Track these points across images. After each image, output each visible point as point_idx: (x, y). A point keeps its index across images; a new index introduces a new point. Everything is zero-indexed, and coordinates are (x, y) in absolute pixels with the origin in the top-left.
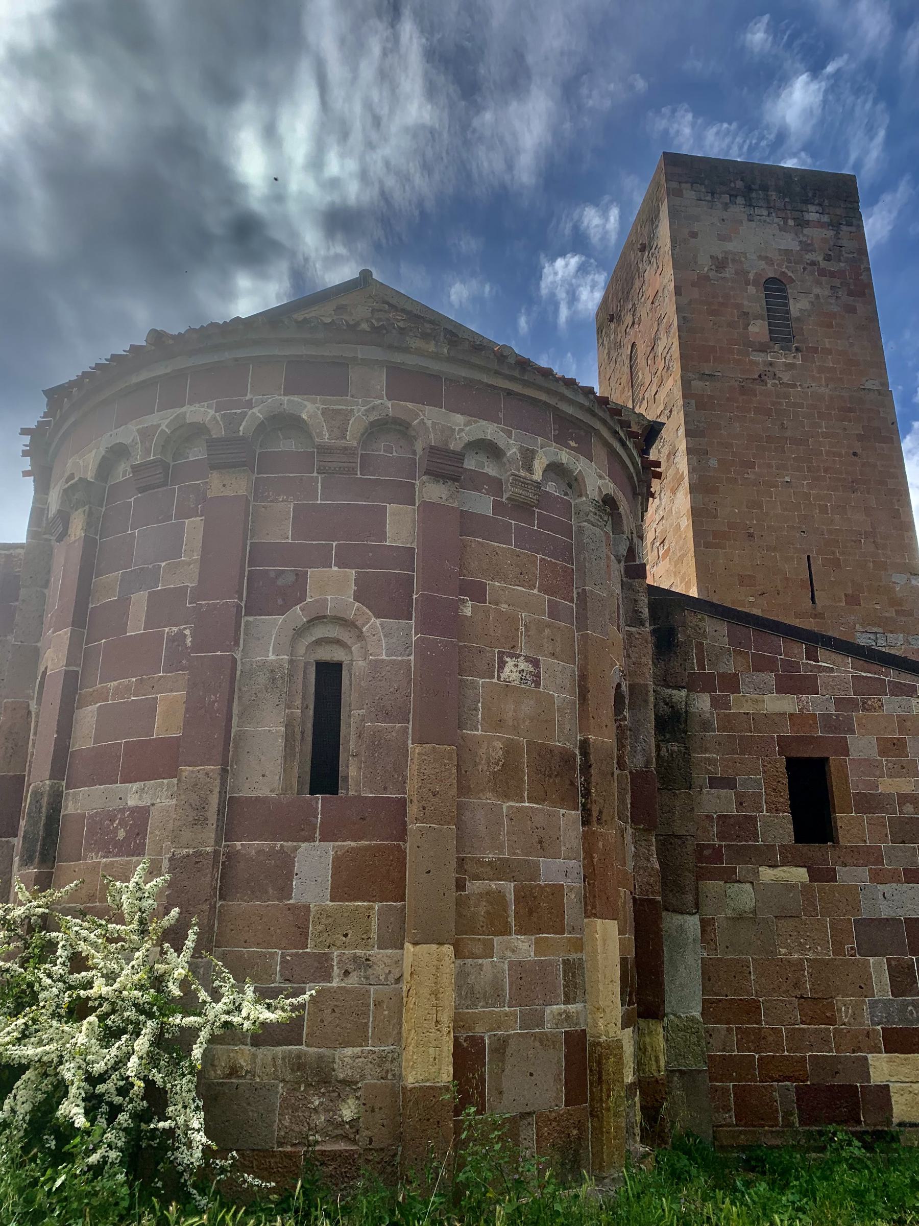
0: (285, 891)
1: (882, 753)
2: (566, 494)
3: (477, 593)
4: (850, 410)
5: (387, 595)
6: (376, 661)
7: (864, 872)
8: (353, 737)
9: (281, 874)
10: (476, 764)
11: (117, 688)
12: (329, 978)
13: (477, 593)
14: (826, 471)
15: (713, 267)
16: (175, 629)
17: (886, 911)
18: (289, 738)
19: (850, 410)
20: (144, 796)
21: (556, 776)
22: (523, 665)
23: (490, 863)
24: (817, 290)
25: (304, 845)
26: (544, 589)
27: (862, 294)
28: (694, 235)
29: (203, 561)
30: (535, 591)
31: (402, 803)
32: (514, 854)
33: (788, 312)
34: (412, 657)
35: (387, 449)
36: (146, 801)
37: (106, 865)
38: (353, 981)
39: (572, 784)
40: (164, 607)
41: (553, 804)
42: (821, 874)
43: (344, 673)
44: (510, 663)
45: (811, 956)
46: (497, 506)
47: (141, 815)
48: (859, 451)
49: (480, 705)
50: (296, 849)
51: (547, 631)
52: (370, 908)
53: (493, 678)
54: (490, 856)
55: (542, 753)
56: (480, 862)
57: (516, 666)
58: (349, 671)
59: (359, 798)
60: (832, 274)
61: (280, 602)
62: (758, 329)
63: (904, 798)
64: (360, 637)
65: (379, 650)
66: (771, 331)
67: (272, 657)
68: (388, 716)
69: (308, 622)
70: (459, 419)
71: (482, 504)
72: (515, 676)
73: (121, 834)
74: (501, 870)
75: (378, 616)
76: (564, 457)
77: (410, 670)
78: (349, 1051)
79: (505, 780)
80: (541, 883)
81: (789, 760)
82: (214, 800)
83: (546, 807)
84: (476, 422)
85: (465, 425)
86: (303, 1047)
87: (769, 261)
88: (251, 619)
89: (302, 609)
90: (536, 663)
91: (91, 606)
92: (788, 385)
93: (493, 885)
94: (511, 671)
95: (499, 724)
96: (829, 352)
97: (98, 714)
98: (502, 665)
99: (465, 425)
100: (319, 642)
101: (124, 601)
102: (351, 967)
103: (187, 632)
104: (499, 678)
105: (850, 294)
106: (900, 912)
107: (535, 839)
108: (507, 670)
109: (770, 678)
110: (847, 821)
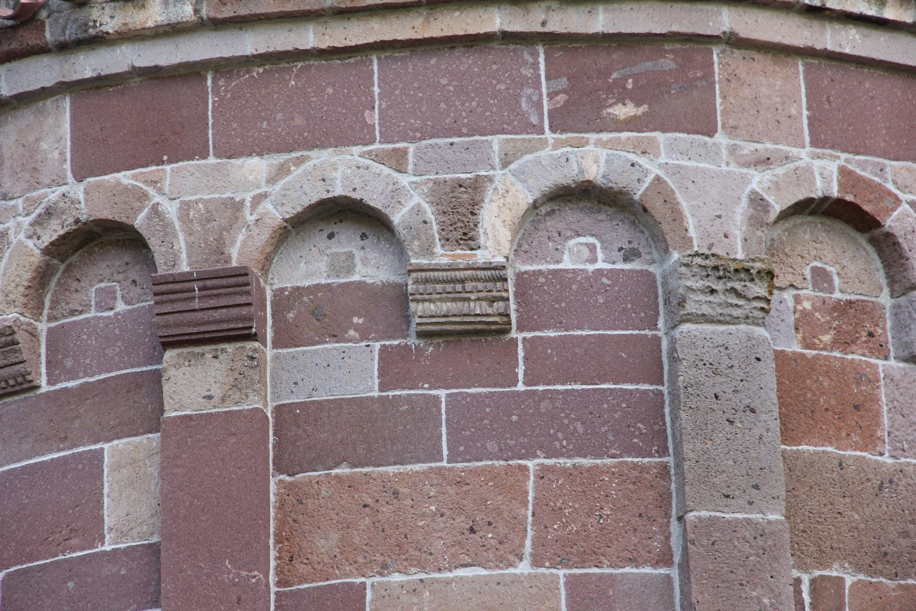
2: (630, 255)
30: (524, 568)
35: (108, 298)
46: (393, 368)
70: (255, 168)
71: (348, 370)
76: (594, 158)
84: (299, 161)
85: (272, 180)
99: (272, 180)
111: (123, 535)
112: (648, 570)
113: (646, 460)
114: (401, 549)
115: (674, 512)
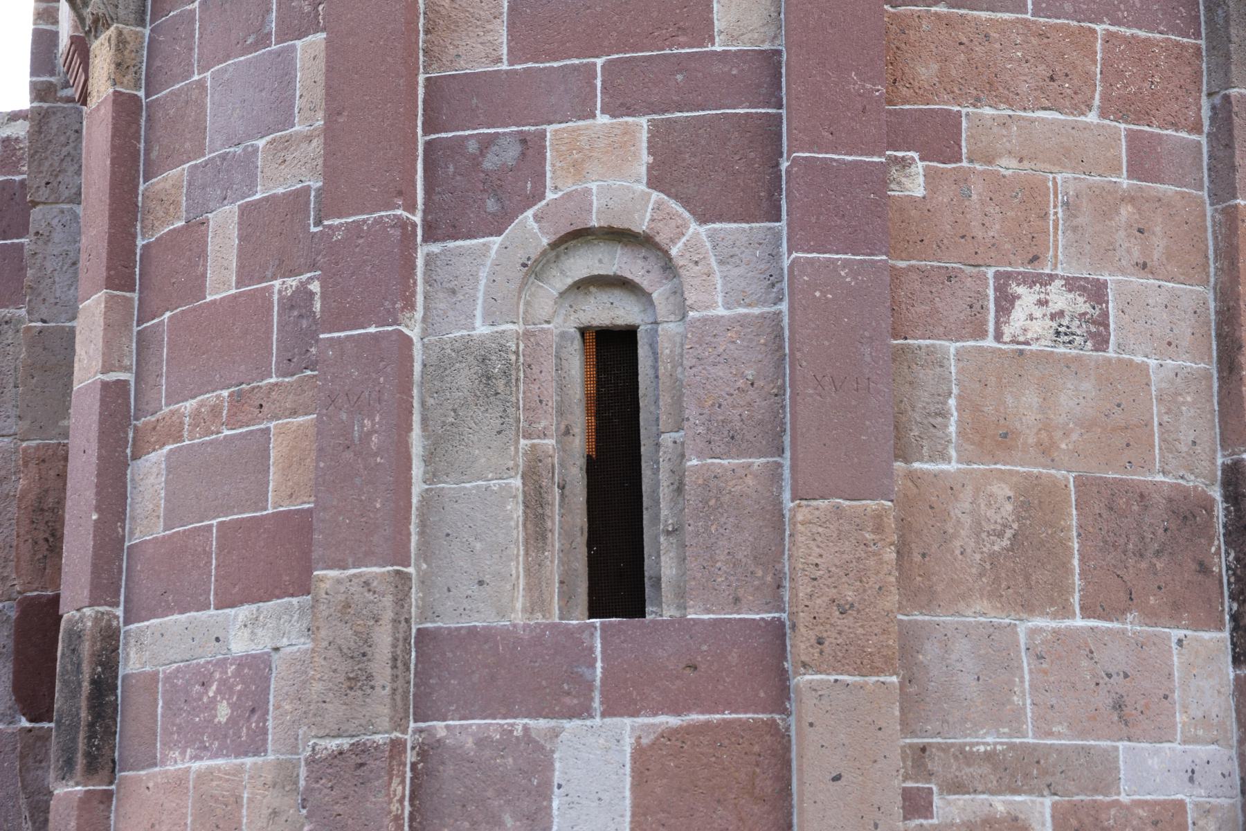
3: (940, 140)
5: (734, 168)
6: (705, 320)
8: (665, 492)
10: (946, 538)
11: (196, 414)
13: (940, 140)
16: (293, 282)
18: (535, 504)
20: (260, 632)
21: (1158, 553)
22: (1060, 299)
23: (989, 757)
25: (571, 726)
26: (1115, 108)
29: (330, 133)
30: (1092, 117)
31: (777, 632)
32: (1050, 734)
34: (784, 307)
37: (200, 776)
39: (1204, 569)
40: (274, 233)
41: (1151, 616)
43: (643, 351)
44: (1027, 297)
47: (256, 670)
49: (952, 402)
50: (555, 734)
51: (1126, 211)
53: (983, 334)
54: (988, 740)
55: (1112, 505)
56: (966, 756)
57: (1042, 303)
58: (653, 346)
59: (682, 624)
61: (491, 205)
64: (669, 267)
65: (712, 292)
67: (482, 329)
68: (734, 442)
69: (554, 245)
72: (1041, 327)
73: (223, 712)
74: (1016, 770)
75: (703, 219)
77: (780, 336)
79: (1025, 569)
80: (1124, 798)
82: (383, 639)
83: (1131, 625)
88: (435, 248)
89: (537, 218)
90: (1096, 292)
91: (140, 242)
93: (1000, 804)
94: (1029, 318)
95: (994, 438)
97: (169, 470)
98: (1006, 303)
100: (586, 284)
101: (196, 226)
103: (315, 287)
104: (998, 337)
107: (1103, 700)
108: (1018, 316)
111: (734, 39)
112: (1184, 135)
113: (1185, 40)
114: (992, 87)
115: (1204, 88)
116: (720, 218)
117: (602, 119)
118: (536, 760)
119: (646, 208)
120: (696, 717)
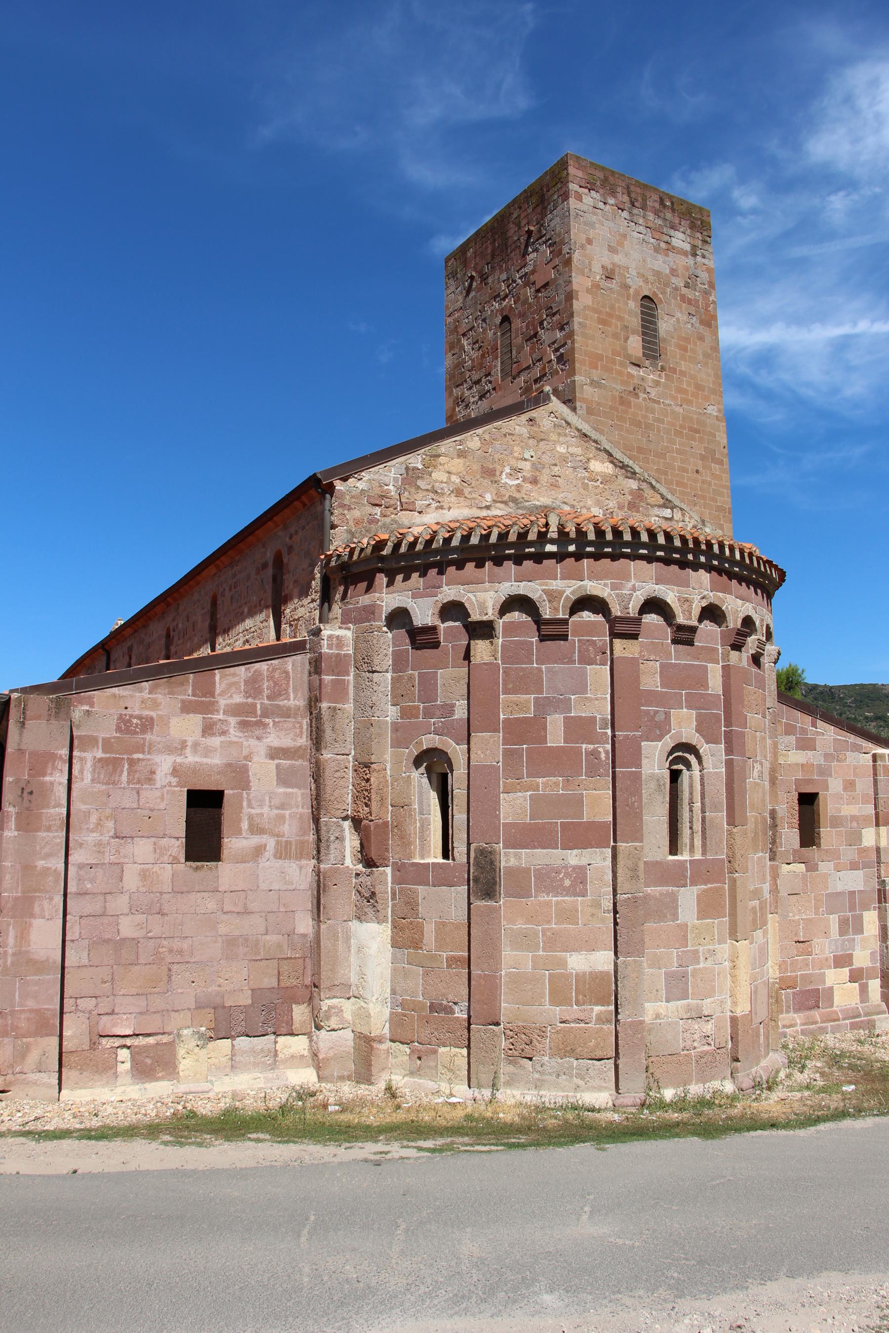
0: (675, 916)
1: (845, 789)
4: (697, 431)
7: (831, 865)
9: (670, 907)
12: (698, 963)
14: (677, 485)
15: (604, 277)
16: (591, 747)
17: (840, 888)
19: (697, 431)
20: (583, 858)
24: (678, 315)
27: (709, 325)
28: (589, 241)
33: (655, 330)
36: (584, 862)
37: (557, 903)
38: (709, 964)
42: (811, 867)
45: (804, 917)
48: (701, 469)
52: (713, 923)
60: (690, 302)
62: (635, 344)
63: (853, 818)
66: (644, 347)
73: (567, 883)
78: (709, 1000)
81: (800, 795)
86: (690, 1000)
87: (646, 281)
89: (670, 738)
92: (654, 401)
96: (683, 373)
102: (707, 956)
105: (702, 322)
106: (846, 887)
109: (792, 739)
110: (826, 832)
116: (711, 743)
117: (685, 710)
118: (674, 899)
119: (695, 739)
120: (709, 886)
